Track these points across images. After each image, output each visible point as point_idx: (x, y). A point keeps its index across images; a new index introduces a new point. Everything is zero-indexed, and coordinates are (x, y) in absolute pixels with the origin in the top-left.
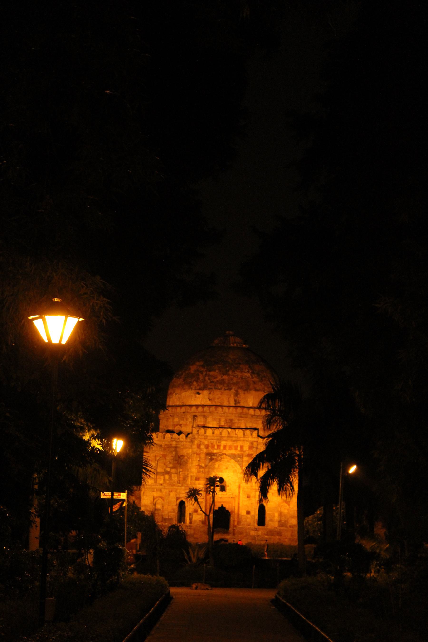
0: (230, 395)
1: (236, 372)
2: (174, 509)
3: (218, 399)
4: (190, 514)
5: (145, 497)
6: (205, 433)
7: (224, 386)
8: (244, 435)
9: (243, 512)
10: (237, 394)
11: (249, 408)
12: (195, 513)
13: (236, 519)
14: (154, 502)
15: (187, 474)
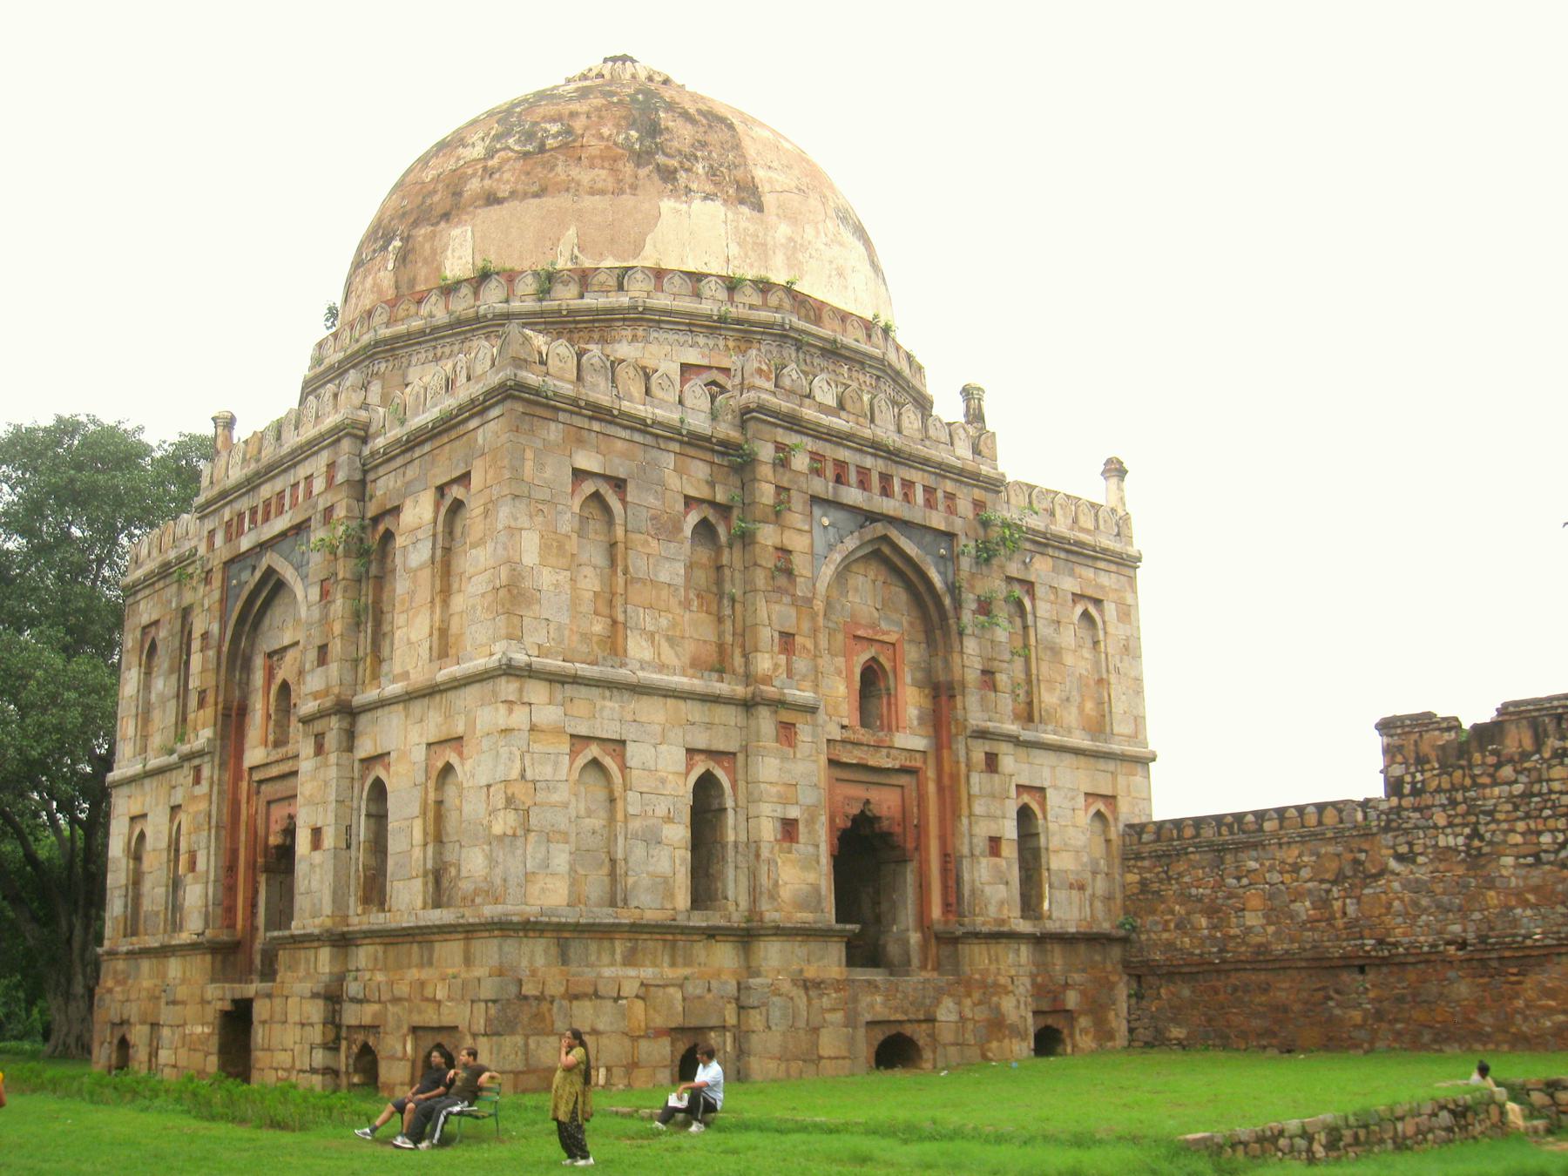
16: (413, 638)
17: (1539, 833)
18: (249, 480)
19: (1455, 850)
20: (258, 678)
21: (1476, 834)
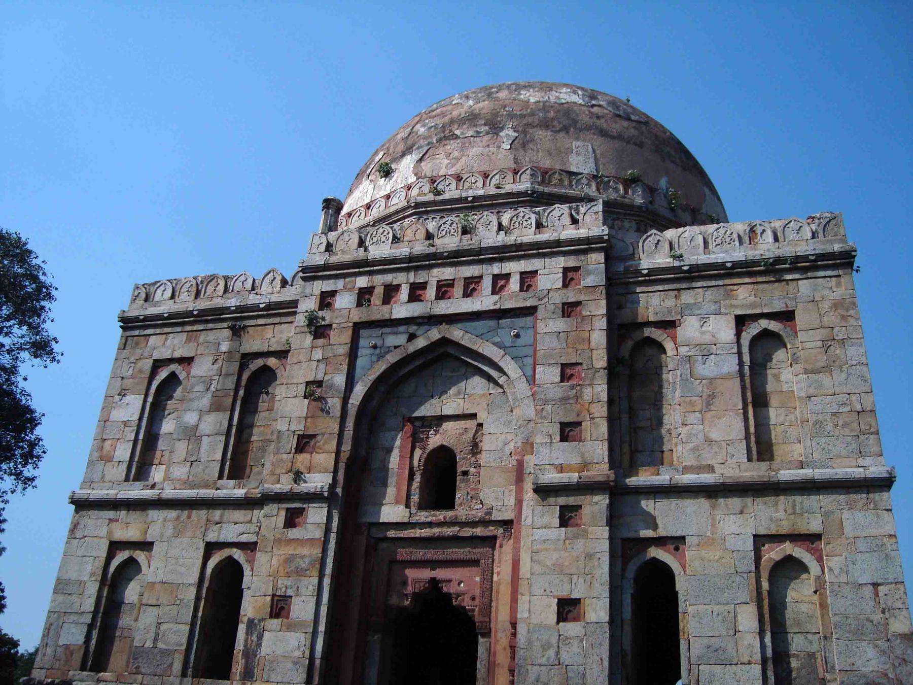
4: (251, 623)
7: (475, 126)
12: (275, 623)
13: (502, 658)
14: (112, 569)
16: (714, 435)
18: (411, 259)
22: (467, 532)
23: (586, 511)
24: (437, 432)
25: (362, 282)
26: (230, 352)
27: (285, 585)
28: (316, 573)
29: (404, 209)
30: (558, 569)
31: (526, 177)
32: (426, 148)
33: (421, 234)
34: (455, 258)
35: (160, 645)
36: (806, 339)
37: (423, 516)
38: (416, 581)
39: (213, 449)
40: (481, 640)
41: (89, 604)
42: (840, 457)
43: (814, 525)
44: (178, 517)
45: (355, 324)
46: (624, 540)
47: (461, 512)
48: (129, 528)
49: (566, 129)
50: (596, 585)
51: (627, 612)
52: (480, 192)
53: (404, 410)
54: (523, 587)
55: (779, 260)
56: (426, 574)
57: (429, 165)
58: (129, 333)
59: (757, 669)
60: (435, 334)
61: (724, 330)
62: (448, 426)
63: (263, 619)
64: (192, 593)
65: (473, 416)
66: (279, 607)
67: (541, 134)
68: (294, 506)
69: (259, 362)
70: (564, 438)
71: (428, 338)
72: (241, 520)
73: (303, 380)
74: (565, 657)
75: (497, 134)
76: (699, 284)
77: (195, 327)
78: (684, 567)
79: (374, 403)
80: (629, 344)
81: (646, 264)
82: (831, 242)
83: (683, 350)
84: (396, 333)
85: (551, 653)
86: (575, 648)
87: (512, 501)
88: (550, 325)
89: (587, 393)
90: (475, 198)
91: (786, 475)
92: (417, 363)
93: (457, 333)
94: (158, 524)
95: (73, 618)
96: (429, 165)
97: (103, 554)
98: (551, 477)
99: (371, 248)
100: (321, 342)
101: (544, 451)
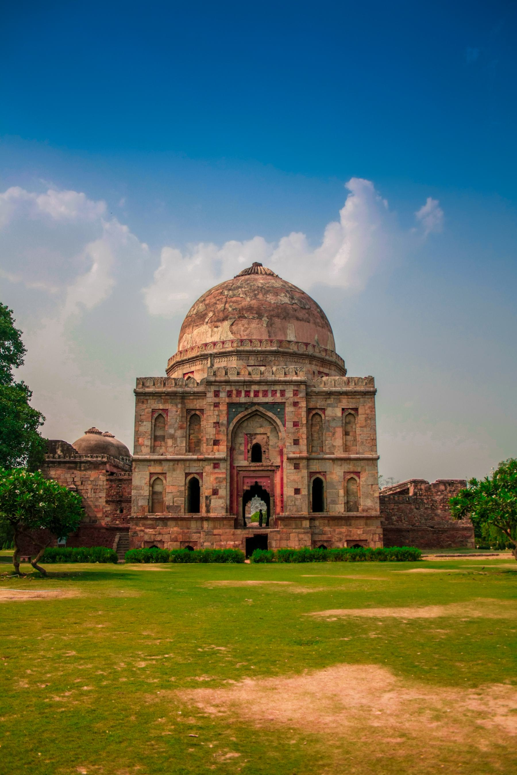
0: (262, 325)
1: (268, 296)
2: (180, 491)
3: (244, 331)
4: (207, 498)
5: (136, 473)
6: (226, 374)
7: (252, 313)
8: (285, 374)
9: (289, 492)
10: (270, 325)
11: (289, 342)
12: (215, 496)
13: (278, 503)
15: (200, 437)
17: (446, 506)
19: (429, 508)
20: (241, 440)
21: (433, 505)
22: (266, 468)
23: (301, 465)
24: (255, 438)
25: (228, 388)
26: (182, 408)
27: (215, 485)
28: (225, 482)
29: (232, 352)
30: (294, 481)
31: (275, 345)
32: (234, 320)
33: (247, 373)
34: (259, 383)
35: (175, 504)
36: (361, 418)
37: (253, 464)
38: (251, 482)
39: (182, 442)
40: (271, 498)
41: (147, 493)
42: (366, 451)
43: (359, 470)
44: (174, 465)
45: (228, 403)
46: (310, 472)
47: (264, 463)
48: (157, 469)
49: (285, 318)
50: (304, 485)
51: (311, 492)
52: (259, 349)
53: (244, 431)
54: (285, 485)
55: (355, 392)
56: (255, 480)
57: (236, 328)
58: (139, 397)
59: (343, 505)
60: (254, 408)
61: (339, 414)
62: (259, 437)
63: (210, 496)
64: (183, 488)
65: (266, 434)
66: (215, 492)
67: (277, 320)
68: (216, 463)
69: (193, 412)
70: (295, 444)
71: (251, 410)
72: (196, 465)
73: (212, 422)
74: (297, 503)
75: (261, 319)
76: (333, 397)
77: (167, 397)
78: (326, 479)
79: (235, 429)
80: (311, 415)
81: (316, 390)
82: (370, 387)
83: (327, 418)
84: (241, 407)
85: (293, 503)
86: (299, 501)
87: (279, 460)
88: (289, 409)
89: (301, 430)
90: (258, 351)
91: (353, 456)
92: (248, 417)
93: (261, 409)
94: (166, 467)
95: (142, 497)
96: (236, 328)
97: (148, 478)
98: (291, 455)
99: (230, 376)
100: (216, 408)
101: (289, 447)
